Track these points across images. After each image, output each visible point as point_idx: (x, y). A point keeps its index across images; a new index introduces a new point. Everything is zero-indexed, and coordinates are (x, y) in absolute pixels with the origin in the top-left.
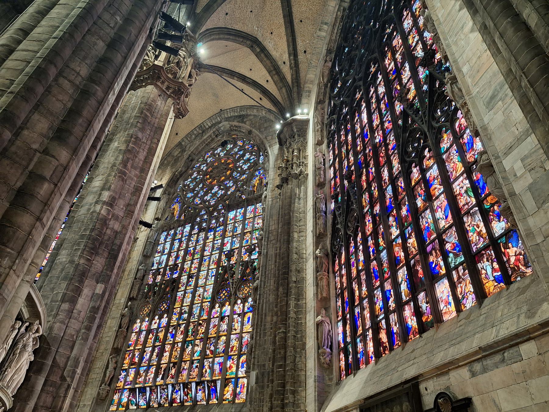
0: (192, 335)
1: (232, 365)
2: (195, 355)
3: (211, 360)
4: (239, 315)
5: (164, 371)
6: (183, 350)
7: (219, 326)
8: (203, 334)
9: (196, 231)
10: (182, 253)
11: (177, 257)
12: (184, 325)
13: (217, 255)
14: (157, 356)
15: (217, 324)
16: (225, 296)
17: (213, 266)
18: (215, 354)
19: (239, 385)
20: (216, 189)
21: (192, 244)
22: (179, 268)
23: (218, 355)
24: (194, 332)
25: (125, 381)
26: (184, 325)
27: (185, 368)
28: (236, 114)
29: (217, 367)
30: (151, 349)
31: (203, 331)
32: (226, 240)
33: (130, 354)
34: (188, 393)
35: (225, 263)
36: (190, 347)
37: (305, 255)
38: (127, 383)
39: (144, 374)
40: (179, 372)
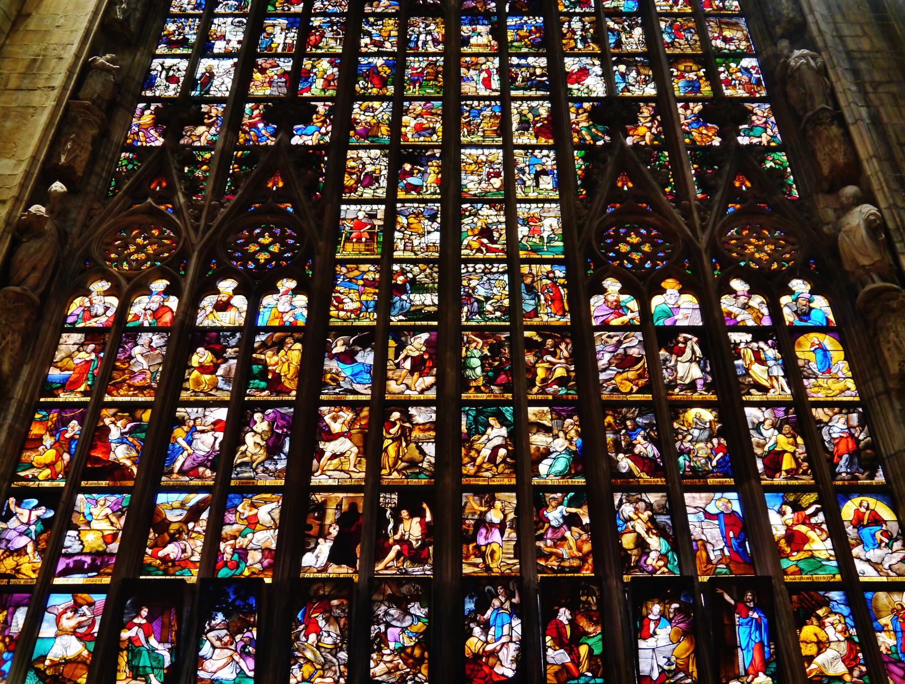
0: (489, 381)
1: (803, 529)
2: (543, 468)
3: (654, 498)
4: (759, 333)
5: (347, 519)
6: (452, 441)
8: (561, 381)
12: (425, 336)
14: (272, 448)
15: (634, 352)
19: (885, 620)
24: (498, 371)
25: (51, 550)
26: (425, 336)
27: (494, 516)
30: (221, 414)
31: (560, 372)
33: (65, 422)
34: (579, 635)
35: (595, 138)
36: (497, 433)
38: (61, 566)
40: (451, 535)
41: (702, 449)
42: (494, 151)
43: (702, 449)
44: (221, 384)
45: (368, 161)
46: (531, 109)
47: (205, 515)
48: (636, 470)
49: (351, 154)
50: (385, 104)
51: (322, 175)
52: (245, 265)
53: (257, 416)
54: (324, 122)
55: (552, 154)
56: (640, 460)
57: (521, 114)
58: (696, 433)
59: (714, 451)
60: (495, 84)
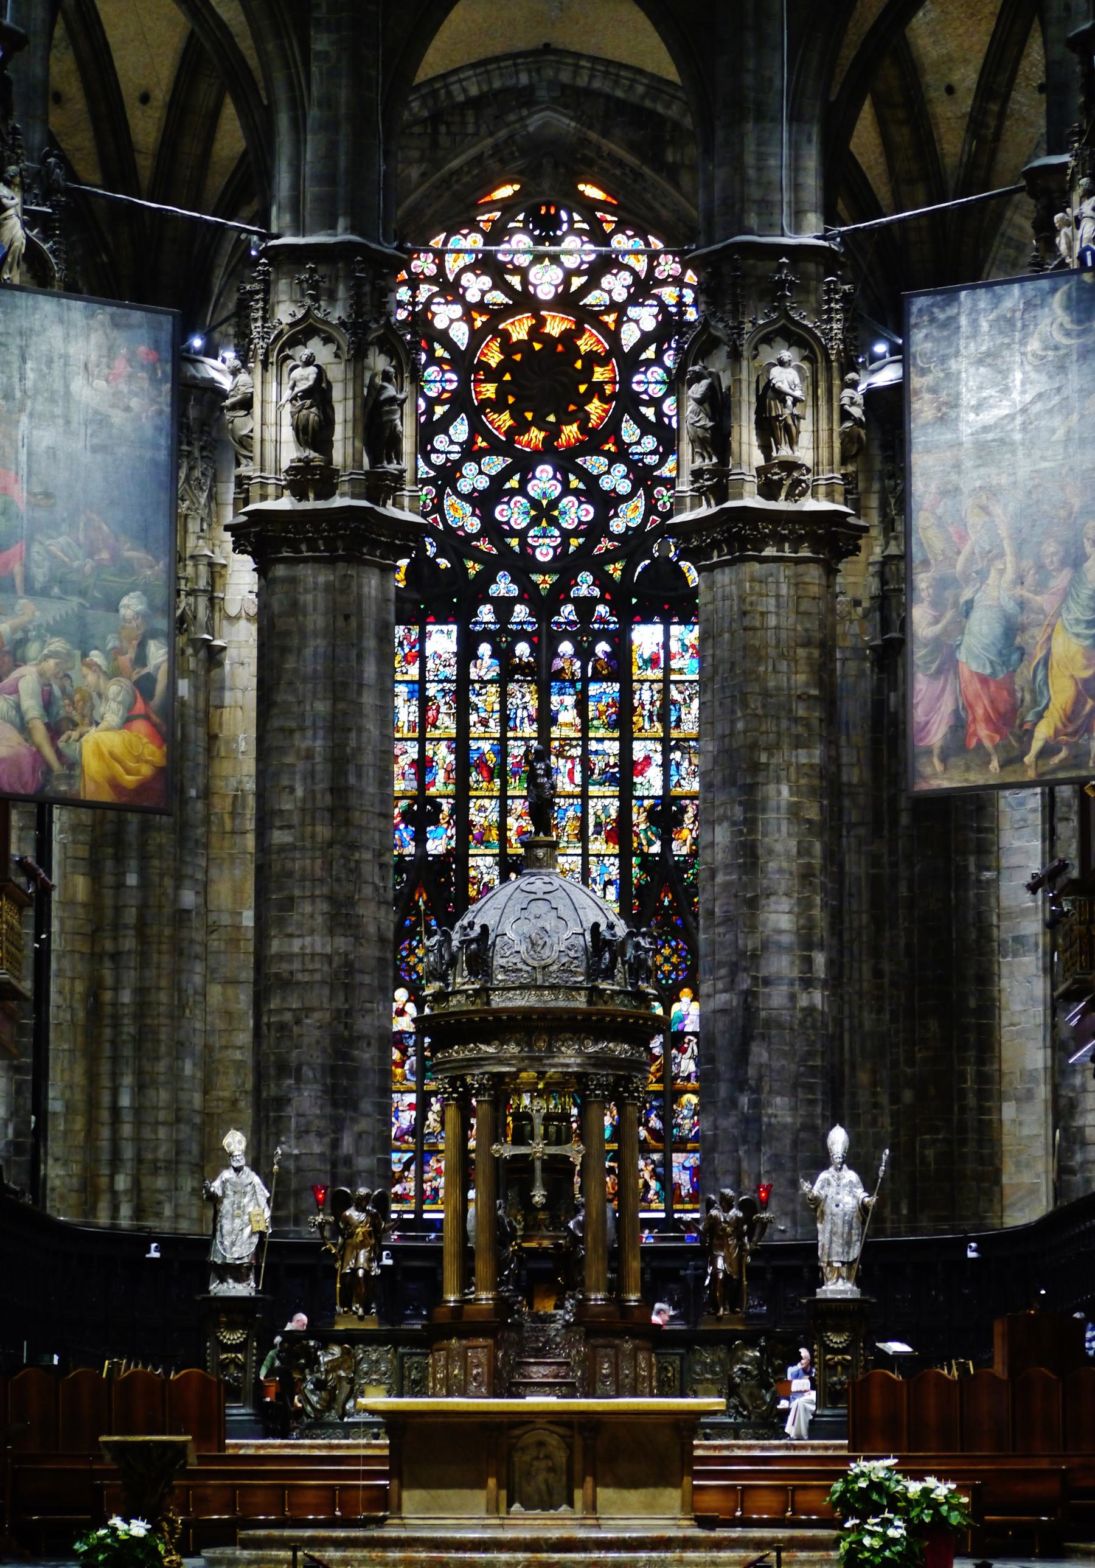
3: (656, 1157)
7: (669, 1060)
9: (485, 666)
10: (443, 755)
11: (423, 765)
13: (614, 806)
16: (675, 967)
17: (597, 846)
18: (668, 1141)
20: (544, 481)
21: (484, 723)
22: (444, 816)
23: (681, 1146)
28: (619, 94)
29: (682, 1178)
30: (412, 1098)
32: (639, 751)
35: (650, 843)
37: (995, 930)
39: (411, 1174)
41: (687, 1124)
42: (575, 858)
43: (687, 1124)
44: (409, 1076)
45: (484, 870)
46: (605, 807)
47: (413, 1168)
48: (649, 1138)
49: (472, 862)
50: (494, 802)
51: (453, 884)
52: (410, 976)
53: (433, 1100)
54: (448, 822)
55: (617, 862)
56: (651, 1131)
57: (597, 817)
58: (685, 1112)
59: (694, 1125)
60: (578, 778)
